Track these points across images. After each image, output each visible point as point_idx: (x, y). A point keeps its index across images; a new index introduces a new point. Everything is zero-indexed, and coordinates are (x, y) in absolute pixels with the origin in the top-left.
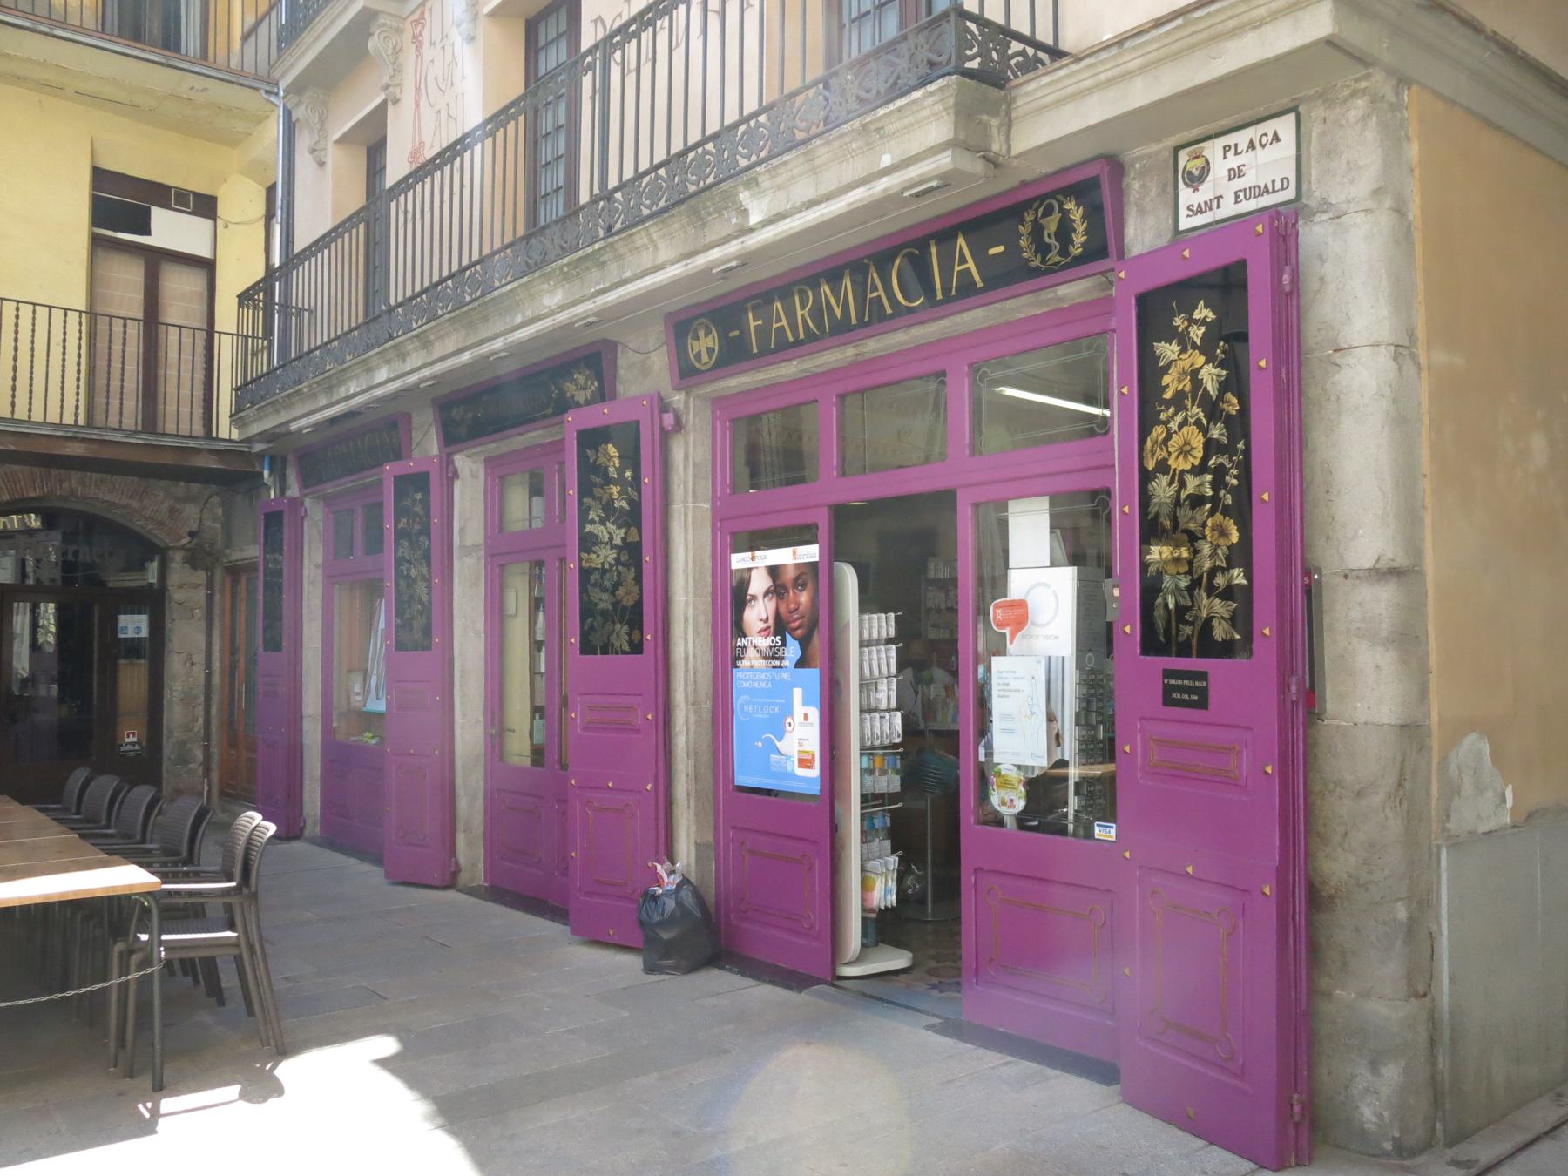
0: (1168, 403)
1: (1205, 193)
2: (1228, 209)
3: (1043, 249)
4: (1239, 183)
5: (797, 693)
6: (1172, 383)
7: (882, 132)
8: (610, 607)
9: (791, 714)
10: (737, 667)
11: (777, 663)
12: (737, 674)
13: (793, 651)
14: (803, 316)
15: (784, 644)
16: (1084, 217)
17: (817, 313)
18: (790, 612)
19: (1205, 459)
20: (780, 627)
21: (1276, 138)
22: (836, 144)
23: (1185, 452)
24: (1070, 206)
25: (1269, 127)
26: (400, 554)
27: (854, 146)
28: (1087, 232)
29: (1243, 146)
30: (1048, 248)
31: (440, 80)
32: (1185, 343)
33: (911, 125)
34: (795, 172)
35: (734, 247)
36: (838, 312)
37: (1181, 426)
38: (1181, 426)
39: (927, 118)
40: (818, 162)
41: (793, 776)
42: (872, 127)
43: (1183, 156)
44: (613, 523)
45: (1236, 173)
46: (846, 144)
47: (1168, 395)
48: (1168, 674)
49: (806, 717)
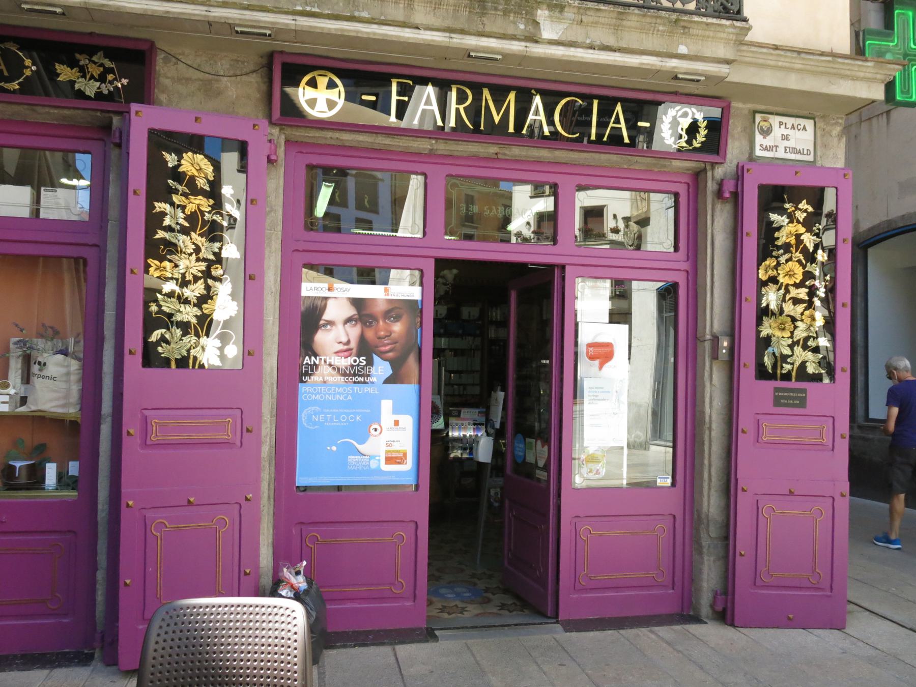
1: (768, 141)
2: (781, 154)
4: (786, 143)
5: (386, 406)
6: (783, 237)
7: (686, 30)
8: (194, 321)
9: (378, 421)
10: (302, 382)
11: (360, 379)
12: (302, 388)
13: (381, 369)
14: (458, 110)
15: (370, 363)
16: (706, 127)
17: (475, 112)
18: (379, 338)
20: (365, 349)
21: (804, 128)
22: (648, 20)
23: (790, 274)
27: (661, 28)
28: (706, 136)
29: (789, 126)
30: (681, 137)
32: (792, 218)
33: (708, 37)
34: (602, 20)
35: (516, 47)
36: (497, 119)
37: (787, 261)
38: (787, 261)
39: (722, 39)
40: (625, 23)
41: (379, 471)
42: (682, 24)
43: (758, 117)
44: (201, 235)
45: (785, 138)
46: (656, 23)
47: (779, 243)
48: (777, 390)
49: (396, 423)
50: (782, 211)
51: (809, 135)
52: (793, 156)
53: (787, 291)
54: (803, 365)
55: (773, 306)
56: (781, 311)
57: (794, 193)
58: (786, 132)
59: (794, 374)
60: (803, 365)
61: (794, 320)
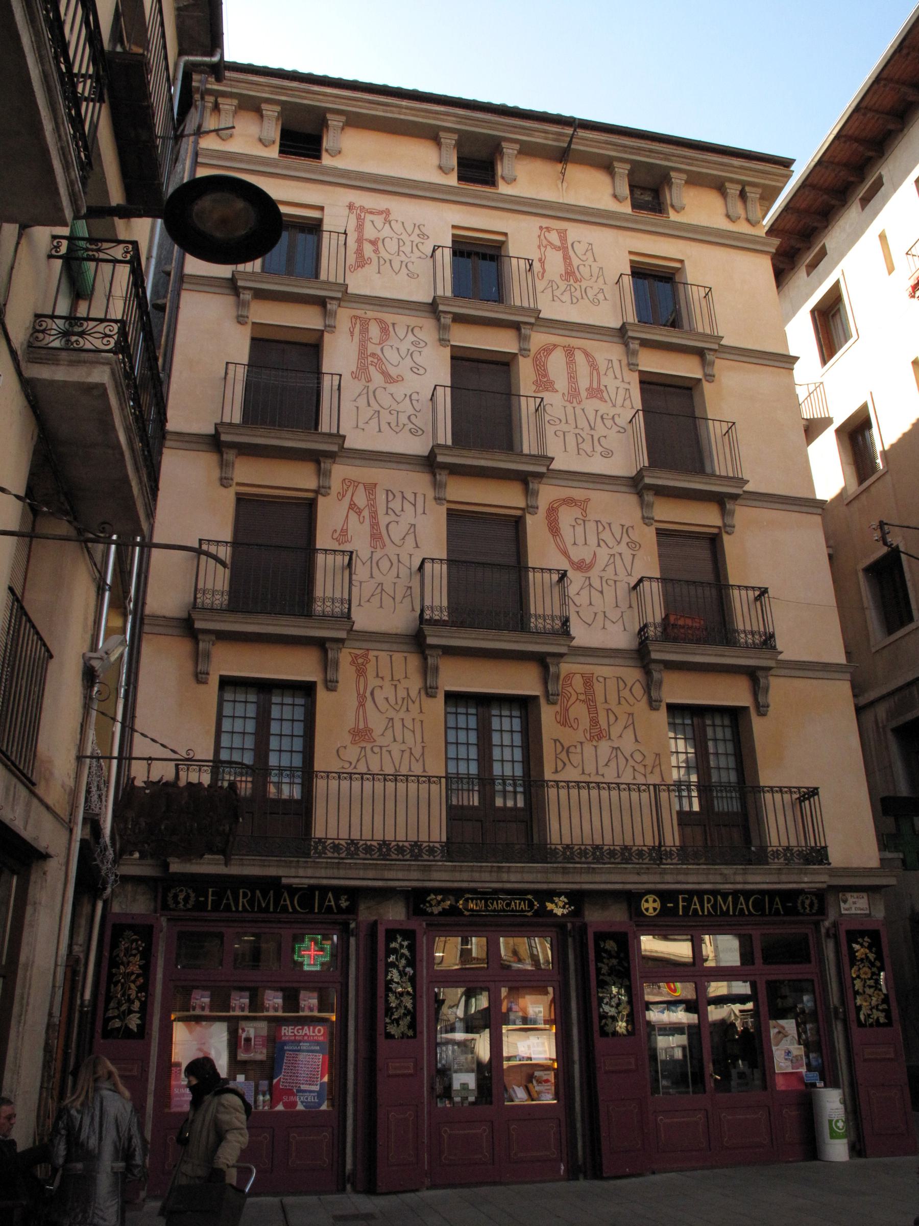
1: (847, 906)
2: (853, 911)
3: (804, 908)
17: (714, 907)
23: (865, 973)
26: (389, 977)
31: (392, 700)
32: (862, 945)
50: (857, 943)
52: (859, 912)
53: (865, 982)
54: (878, 1019)
55: (861, 991)
56: (864, 992)
57: (863, 933)
60: (878, 1019)
61: (870, 996)
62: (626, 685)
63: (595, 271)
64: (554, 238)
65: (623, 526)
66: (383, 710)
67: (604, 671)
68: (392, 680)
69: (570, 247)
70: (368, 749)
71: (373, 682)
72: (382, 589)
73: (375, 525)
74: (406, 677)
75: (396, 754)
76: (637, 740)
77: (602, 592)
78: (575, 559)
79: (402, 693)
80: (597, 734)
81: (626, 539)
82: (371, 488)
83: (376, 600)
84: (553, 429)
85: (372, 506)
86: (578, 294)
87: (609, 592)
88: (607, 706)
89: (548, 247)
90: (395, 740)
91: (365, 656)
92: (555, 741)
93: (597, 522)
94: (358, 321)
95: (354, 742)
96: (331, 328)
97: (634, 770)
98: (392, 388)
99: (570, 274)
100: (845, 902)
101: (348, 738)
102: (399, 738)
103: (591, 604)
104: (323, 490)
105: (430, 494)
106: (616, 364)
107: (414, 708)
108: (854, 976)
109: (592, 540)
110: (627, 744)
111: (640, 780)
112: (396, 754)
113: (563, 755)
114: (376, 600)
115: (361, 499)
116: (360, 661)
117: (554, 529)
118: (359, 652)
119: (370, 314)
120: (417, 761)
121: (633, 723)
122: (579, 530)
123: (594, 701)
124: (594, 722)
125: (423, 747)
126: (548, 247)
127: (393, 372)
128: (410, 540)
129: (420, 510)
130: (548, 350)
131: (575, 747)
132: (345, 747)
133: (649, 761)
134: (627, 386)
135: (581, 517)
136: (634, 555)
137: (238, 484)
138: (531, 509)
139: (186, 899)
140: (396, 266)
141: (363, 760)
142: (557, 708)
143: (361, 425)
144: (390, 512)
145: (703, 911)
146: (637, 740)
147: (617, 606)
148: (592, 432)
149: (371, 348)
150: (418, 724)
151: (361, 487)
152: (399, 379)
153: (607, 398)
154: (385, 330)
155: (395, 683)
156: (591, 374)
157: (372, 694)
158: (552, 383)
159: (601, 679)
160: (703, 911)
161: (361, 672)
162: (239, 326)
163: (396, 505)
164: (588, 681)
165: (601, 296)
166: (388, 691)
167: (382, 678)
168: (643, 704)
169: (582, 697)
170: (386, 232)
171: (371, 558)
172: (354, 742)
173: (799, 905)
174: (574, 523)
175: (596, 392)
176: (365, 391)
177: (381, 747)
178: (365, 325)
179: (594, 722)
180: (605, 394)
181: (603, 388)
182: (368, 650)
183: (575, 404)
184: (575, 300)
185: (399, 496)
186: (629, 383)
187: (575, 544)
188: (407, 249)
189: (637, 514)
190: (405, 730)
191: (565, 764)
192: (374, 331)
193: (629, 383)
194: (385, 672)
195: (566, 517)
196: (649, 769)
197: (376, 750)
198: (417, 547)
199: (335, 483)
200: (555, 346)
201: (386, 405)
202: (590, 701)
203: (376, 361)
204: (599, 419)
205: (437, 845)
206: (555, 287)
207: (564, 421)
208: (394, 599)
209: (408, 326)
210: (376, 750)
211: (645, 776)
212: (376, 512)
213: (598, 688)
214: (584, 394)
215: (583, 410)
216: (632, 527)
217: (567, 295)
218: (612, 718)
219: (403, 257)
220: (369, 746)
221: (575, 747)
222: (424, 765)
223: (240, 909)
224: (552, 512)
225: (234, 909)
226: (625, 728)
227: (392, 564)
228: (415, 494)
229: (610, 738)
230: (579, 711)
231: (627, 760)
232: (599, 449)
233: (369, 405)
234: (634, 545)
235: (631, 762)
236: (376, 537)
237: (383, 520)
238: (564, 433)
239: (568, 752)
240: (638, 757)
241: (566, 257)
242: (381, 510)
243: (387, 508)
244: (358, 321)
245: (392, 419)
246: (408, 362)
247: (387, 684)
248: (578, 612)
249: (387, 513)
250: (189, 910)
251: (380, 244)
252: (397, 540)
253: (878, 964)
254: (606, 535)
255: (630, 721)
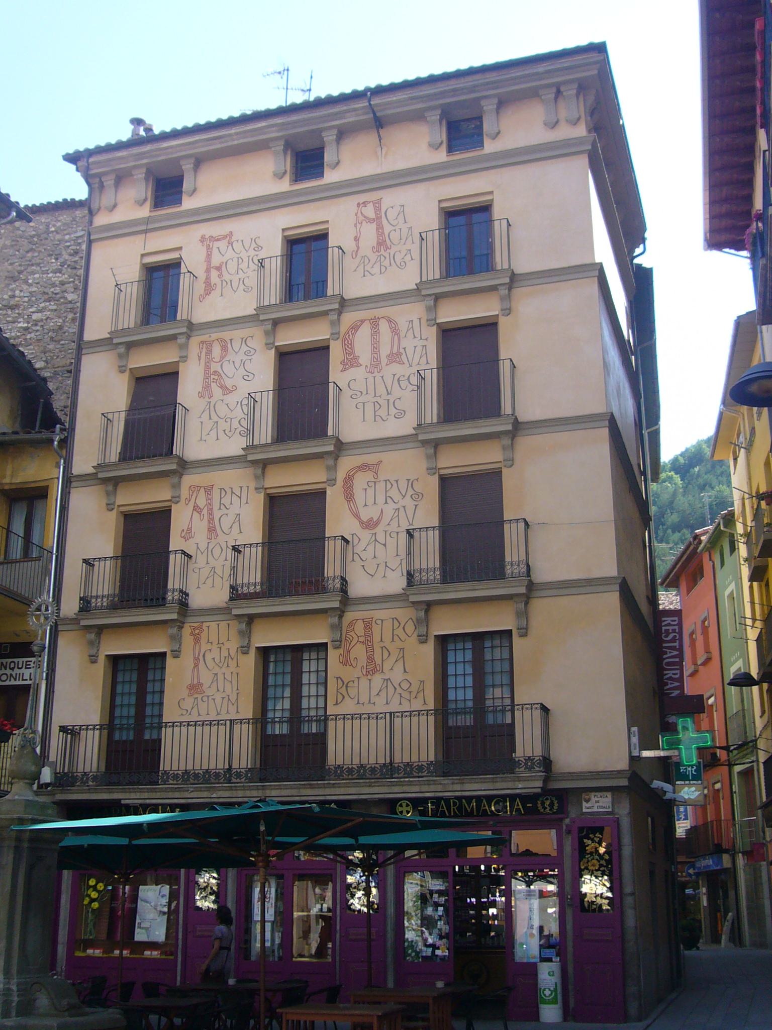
0: (588, 854)
1: (589, 805)
2: (595, 809)
4: (598, 804)
14: (454, 809)
19: (599, 868)
21: (607, 797)
24: (554, 799)
25: (605, 794)
28: (558, 807)
29: (599, 796)
30: (546, 808)
31: (217, 660)
32: (593, 841)
36: (469, 810)
37: (592, 860)
38: (592, 860)
47: (588, 852)
50: (589, 838)
51: (609, 799)
52: (601, 810)
58: (597, 799)
59: (597, 909)
62: (400, 623)
63: (405, 231)
64: (370, 211)
65: (408, 480)
66: (211, 668)
67: (382, 614)
68: (218, 643)
69: (383, 215)
70: (199, 699)
71: (204, 647)
72: (214, 572)
73: (211, 520)
74: (228, 640)
75: (218, 701)
76: (405, 671)
77: (385, 545)
78: (365, 518)
79: (225, 653)
80: (372, 669)
81: (410, 492)
82: (209, 490)
83: (210, 581)
84: (355, 402)
85: (210, 505)
86: (386, 263)
87: (391, 543)
88: (382, 644)
89: (364, 223)
90: (218, 690)
91: (200, 627)
92: (337, 678)
93: (386, 481)
94: (205, 345)
95: (190, 695)
96: (184, 358)
97: (401, 696)
98: (229, 399)
99: (382, 244)
100: (588, 801)
101: (185, 692)
102: (221, 689)
103: (375, 557)
104: (174, 500)
105: (252, 485)
106: (416, 323)
107: (233, 664)
108: (582, 867)
109: (381, 499)
110: (397, 675)
111: (406, 707)
112: (218, 701)
113: (343, 691)
114: (210, 581)
115: (202, 501)
116: (197, 631)
117: (349, 496)
118: (196, 625)
119: (214, 336)
120: (233, 704)
121: (403, 656)
122: (371, 492)
123: (372, 641)
124: (371, 659)
125: (238, 693)
126: (364, 223)
127: (229, 383)
128: (236, 527)
129: (244, 500)
130: (355, 328)
131: (353, 681)
132: (184, 699)
133: (414, 689)
134: (424, 343)
135: (373, 480)
136: (416, 506)
137: (119, 506)
138: (332, 481)
139: (552, 805)
140: (235, 285)
141: (195, 709)
142: (341, 651)
143: (204, 438)
144: (222, 507)
145: (449, 812)
146: (405, 671)
147: (397, 555)
148: (389, 397)
149: (215, 367)
150: (235, 676)
151: (202, 490)
152: (235, 388)
153: (405, 361)
154: (224, 348)
155: (219, 646)
156: (393, 339)
157: (204, 656)
158: (356, 358)
159: (379, 622)
160: (449, 812)
161: (197, 640)
162: (122, 374)
163: (226, 501)
164: (368, 625)
165: (408, 257)
166: (215, 653)
167: (211, 643)
168: (414, 639)
169: (362, 639)
170: (230, 254)
171: (208, 547)
172: (190, 695)
173: (539, 805)
174: (366, 487)
175: (395, 357)
176: (208, 407)
177: (208, 696)
178: (209, 345)
179: (371, 659)
180: (404, 357)
181: (402, 351)
182: (203, 622)
183: (376, 374)
184: (383, 269)
185: (229, 491)
186: (426, 339)
187: (366, 505)
188: (244, 266)
189: (423, 465)
190: (226, 680)
191: (344, 697)
192: (217, 350)
193: (426, 339)
194: (213, 638)
195: (360, 481)
196: (413, 695)
197: (205, 699)
198: (241, 532)
199: (184, 492)
200: (363, 321)
201: (222, 415)
202: (368, 642)
203: (216, 377)
204: (396, 382)
205: (221, 771)
206: (367, 261)
207: (364, 393)
208: (222, 578)
209: (242, 339)
210: (205, 699)
211: (410, 701)
212: (212, 509)
213: (376, 629)
214: (384, 361)
215: (382, 377)
216: (417, 480)
217: (377, 266)
218: (386, 654)
219: (241, 275)
220: (200, 697)
221: (353, 681)
222: (237, 708)
223: (452, 814)
224: (349, 479)
225: (447, 815)
226: (396, 661)
227: (222, 550)
228: (241, 487)
229: (382, 672)
230: (359, 652)
231: (395, 689)
232: (393, 411)
233: (210, 419)
234: (418, 496)
235: (399, 690)
236: (212, 530)
237: (217, 514)
238: (364, 403)
239: (347, 687)
240: (405, 685)
241: (380, 228)
242: (216, 506)
243: (220, 504)
244: (205, 345)
245: (226, 426)
246: (242, 372)
247: (215, 647)
248: (363, 566)
249: (220, 509)
250: (554, 813)
251: (224, 268)
252: (226, 530)
253: (607, 857)
254: (394, 493)
255: (401, 655)
